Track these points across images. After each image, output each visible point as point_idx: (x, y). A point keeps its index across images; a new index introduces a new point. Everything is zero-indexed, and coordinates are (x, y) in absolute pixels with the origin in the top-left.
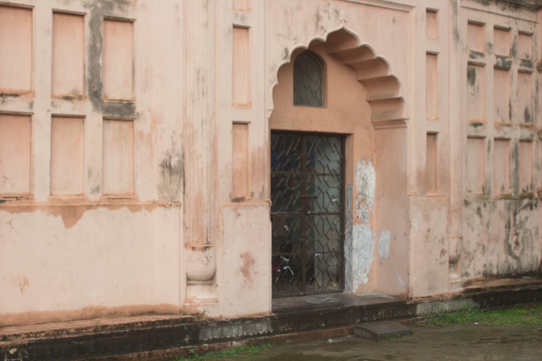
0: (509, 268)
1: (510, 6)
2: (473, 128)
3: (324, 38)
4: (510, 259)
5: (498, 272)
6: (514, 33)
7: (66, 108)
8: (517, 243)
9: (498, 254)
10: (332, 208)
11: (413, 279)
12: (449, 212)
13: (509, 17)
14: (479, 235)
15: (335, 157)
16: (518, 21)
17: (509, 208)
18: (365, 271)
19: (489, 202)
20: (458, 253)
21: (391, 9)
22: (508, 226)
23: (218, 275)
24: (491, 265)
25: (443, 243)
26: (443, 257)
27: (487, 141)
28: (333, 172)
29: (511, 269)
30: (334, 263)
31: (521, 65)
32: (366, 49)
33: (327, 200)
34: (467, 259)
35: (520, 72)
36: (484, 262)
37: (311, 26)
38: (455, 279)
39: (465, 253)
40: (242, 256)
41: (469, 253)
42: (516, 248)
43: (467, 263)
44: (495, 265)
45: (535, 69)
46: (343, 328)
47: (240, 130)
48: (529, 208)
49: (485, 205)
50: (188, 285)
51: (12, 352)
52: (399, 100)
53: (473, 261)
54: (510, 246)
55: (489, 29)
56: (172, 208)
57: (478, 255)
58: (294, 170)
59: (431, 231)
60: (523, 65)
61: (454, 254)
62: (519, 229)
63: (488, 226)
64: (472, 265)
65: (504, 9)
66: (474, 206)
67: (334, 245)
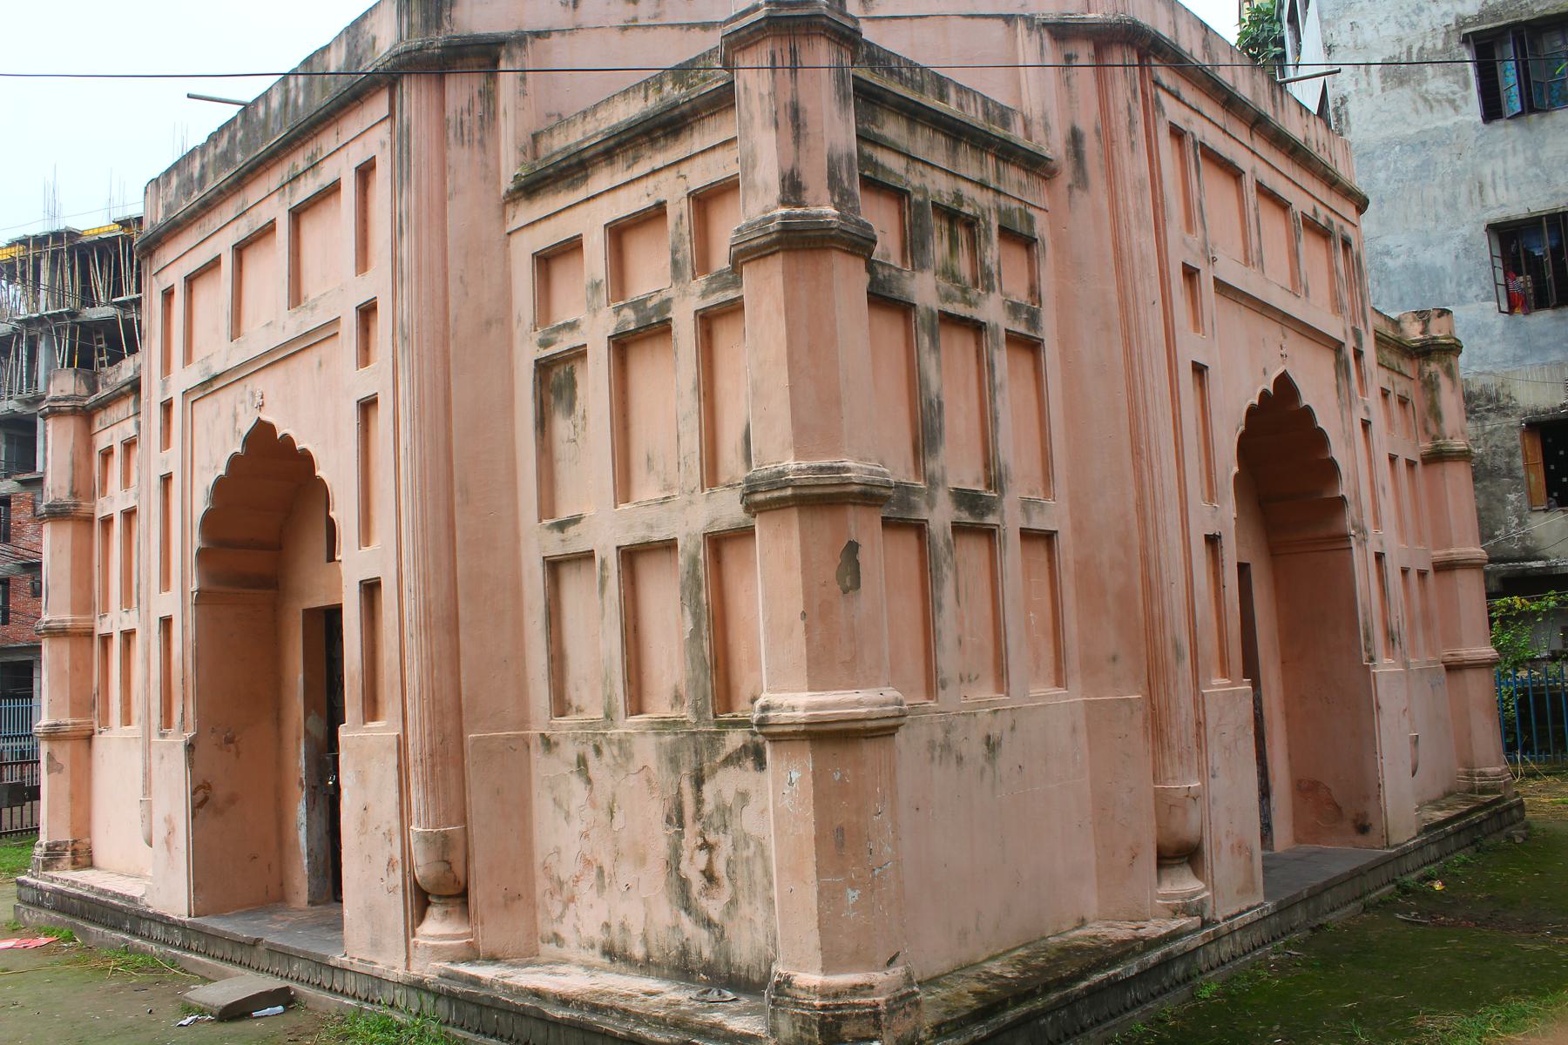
0: (684, 953)
1: (653, 141)
2: (557, 535)
4: (687, 924)
5: (648, 956)
6: (678, 207)
8: (710, 876)
9: (645, 901)
13: (654, 172)
14: (585, 835)
16: (685, 169)
17: (674, 762)
19: (610, 742)
21: (315, 343)
22: (676, 817)
24: (624, 928)
25: (390, 840)
26: (392, 874)
29: (694, 957)
32: (288, 440)
34: (557, 897)
36: (604, 918)
39: (551, 878)
41: (561, 883)
43: (557, 909)
44: (637, 930)
48: (749, 764)
49: (598, 751)
53: (572, 906)
54: (684, 884)
57: (586, 891)
59: (369, 809)
60: (714, 292)
62: (716, 831)
63: (612, 812)
64: (569, 920)
65: (636, 160)
66: (570, 751)
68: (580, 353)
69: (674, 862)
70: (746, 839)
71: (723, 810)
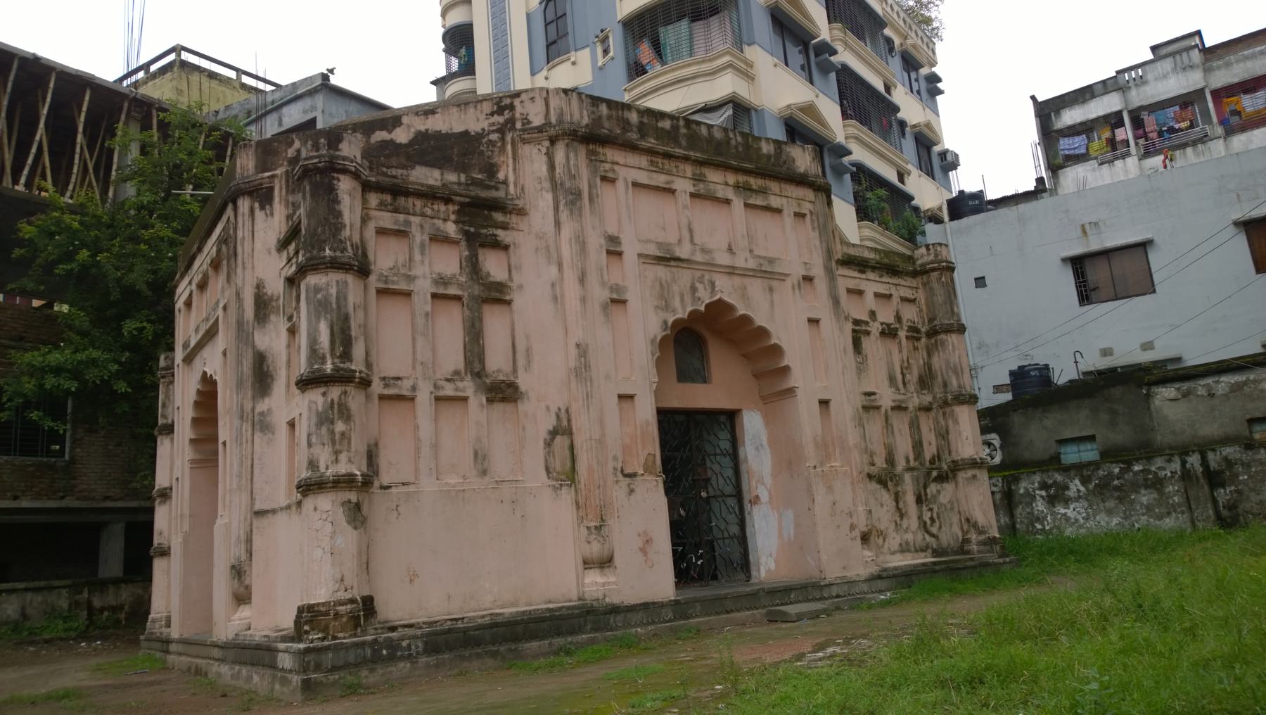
1: (887, 273)
3: (702, 308)
4: (927, 536)
6: (896, 300)
7: (449, 390)
8: (932, 519)
10: (729, 490)
11: (824, 557)
12: (852, 483)
15: (724, 435)
16: (898, 288)
18: (771, 556)
20: (870, 527)
23: (616, 555)
26: (853, 532)
27: (883, 410)
28: (725, 452)
30: (735, 552)
31: (908, 331)
32: (746, 319)
33: (721, 481)
35: (907, 337)
36: (899, 542)
37: (688, 298)
38: (869, 557)
40: (639, 535)
41: (882, 532)
42: (932, 525)
45: (924, 335)
46: (755, 612)
47: (626, 405)
50: (585, 569)
51: (404, 644)
52: (786, 370)
54: (925, 523)
55: (869, 296)
56: (563, 488)
58: (684, 451)
61: (865, 529)
64: (886, 545)
65: (881, 276)
67: (734, 529)
68: (868, 333)
69: (920, 517)
70: (941, 504)
71: (934, 497)
